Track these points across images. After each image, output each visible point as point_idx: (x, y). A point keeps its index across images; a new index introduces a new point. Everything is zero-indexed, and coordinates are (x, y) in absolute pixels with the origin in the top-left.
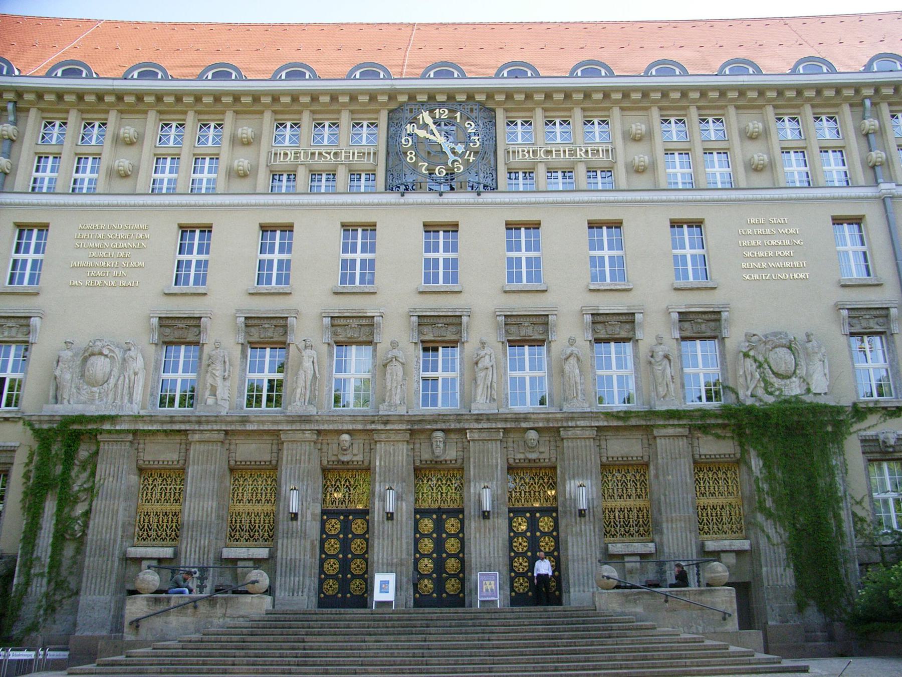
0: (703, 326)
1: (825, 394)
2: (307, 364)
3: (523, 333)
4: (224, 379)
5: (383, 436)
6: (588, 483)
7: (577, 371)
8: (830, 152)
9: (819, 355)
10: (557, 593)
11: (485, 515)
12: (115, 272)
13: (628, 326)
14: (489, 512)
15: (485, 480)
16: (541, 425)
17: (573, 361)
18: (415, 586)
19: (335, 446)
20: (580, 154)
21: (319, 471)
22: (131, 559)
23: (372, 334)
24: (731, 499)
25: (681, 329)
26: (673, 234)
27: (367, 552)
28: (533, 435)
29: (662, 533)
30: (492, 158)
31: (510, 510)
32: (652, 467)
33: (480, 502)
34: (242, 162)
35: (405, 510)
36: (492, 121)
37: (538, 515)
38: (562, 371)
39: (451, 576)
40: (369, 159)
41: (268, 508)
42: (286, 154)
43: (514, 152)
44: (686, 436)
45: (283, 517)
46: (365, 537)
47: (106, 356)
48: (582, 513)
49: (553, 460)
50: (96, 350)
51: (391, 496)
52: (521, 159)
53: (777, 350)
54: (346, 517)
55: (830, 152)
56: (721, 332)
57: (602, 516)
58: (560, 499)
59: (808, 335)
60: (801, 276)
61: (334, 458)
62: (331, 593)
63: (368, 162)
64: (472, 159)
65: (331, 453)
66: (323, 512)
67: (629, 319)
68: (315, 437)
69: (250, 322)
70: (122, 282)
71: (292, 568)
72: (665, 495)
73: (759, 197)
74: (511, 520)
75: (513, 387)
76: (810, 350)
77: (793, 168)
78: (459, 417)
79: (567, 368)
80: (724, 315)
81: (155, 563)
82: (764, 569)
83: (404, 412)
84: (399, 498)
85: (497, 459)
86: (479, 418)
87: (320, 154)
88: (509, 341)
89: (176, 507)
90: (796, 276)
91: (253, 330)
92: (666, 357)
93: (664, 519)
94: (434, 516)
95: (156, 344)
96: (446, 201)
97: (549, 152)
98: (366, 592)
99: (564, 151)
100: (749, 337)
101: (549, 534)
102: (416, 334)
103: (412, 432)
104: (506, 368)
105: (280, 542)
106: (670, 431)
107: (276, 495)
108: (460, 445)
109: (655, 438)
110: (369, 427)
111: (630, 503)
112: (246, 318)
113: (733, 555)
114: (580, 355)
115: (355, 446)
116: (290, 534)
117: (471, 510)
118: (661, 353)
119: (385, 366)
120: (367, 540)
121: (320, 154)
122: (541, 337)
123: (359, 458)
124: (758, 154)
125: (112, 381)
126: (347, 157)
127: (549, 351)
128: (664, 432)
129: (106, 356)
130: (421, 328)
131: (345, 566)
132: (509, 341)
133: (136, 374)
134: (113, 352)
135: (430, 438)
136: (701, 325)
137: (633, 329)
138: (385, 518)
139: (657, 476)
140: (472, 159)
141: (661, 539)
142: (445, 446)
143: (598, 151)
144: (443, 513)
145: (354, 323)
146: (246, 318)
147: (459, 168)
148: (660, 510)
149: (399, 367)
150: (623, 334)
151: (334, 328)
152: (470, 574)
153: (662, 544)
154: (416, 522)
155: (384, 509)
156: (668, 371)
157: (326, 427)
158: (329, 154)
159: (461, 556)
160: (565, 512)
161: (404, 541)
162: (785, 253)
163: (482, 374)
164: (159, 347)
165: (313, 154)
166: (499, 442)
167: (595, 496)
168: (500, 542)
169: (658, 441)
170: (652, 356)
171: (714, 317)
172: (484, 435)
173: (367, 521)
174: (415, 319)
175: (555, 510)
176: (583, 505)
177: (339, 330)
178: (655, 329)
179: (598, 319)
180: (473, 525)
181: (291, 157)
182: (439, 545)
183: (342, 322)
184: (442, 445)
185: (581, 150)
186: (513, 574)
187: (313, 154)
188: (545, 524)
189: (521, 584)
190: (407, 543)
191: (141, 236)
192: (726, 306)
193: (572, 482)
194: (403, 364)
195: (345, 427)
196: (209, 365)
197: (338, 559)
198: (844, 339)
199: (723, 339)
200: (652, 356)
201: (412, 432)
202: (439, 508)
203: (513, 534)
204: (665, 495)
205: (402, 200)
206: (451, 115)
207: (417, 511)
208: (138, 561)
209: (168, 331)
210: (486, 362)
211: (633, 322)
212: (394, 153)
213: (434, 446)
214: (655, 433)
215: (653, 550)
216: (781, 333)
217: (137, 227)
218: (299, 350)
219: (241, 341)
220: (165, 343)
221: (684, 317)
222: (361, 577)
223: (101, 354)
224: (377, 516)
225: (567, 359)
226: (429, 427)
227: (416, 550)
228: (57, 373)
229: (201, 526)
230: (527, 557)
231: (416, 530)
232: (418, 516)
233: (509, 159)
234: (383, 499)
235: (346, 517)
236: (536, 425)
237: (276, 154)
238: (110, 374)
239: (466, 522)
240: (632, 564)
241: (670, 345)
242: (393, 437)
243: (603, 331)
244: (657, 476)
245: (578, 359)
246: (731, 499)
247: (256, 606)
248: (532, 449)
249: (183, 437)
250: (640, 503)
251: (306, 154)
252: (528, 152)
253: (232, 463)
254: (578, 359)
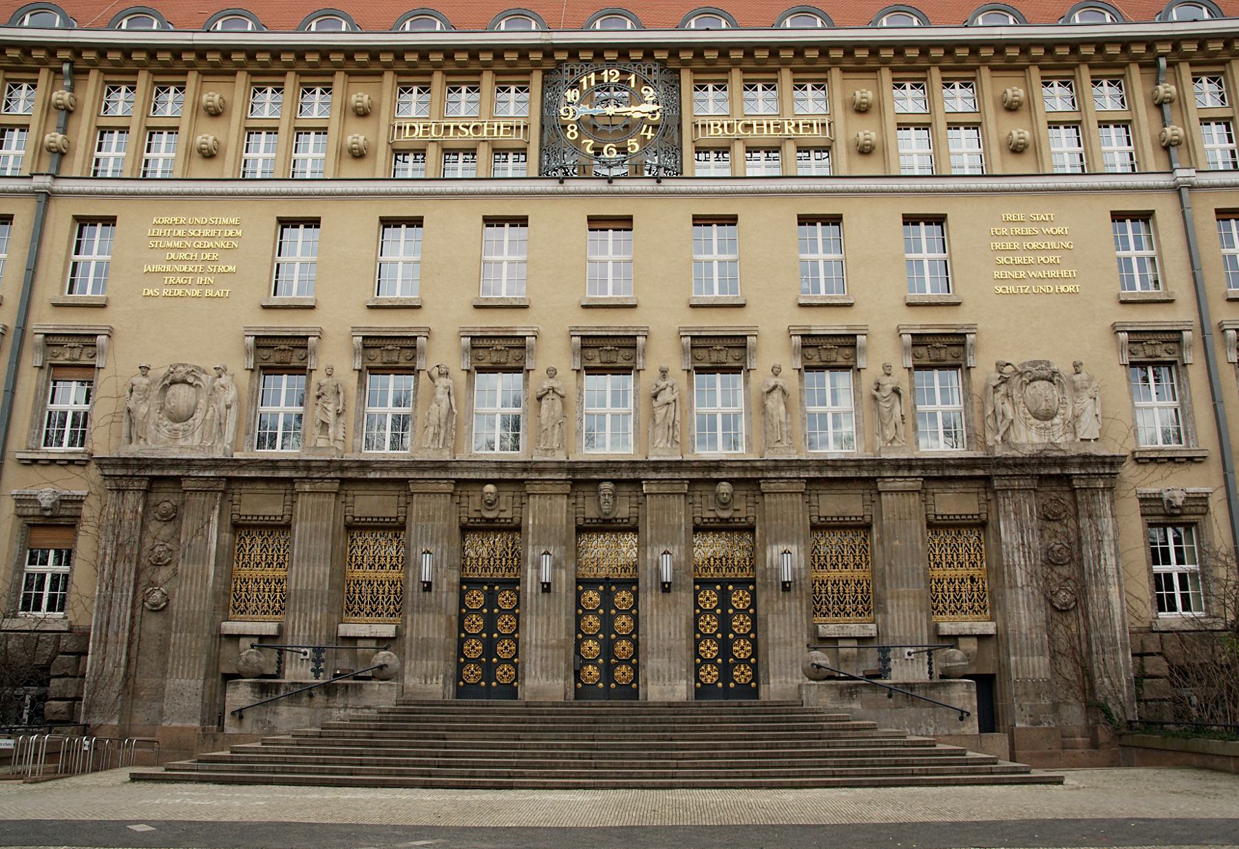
0: (943, 352)
1: (1096, 440)
2: (441, 395)
3: (714, 359)
4: (338, 415)
5: (537, 487)
6: (794, 549)
7: (782, 408)
8: (1112, 127)
9: (1090, 392)
10: (753, 684)
11: (666, 588)
12: (200, 280)
13: (847, 351)
14: (669, 584)
15: (660, 542)
16: (736, 475)
17: (776, 395)
18: (577, 674)
19: (478, 498)
20: (789, 129)
21: (457, 530)
22: (227, 636)
23: (523, 358)
24: (973, 571)
25: (914, 356)
26: (906, 233)
27: (517, 631)
28: (725, 488)
29: (886, 612)
30: (676, 134)
31: (696, 582)
32: (874, 529)
33: (658, 571)
34: (357, 135)
35: (564, 580)
36: (676, 84)
37: (731, 587)
38: (764, 406)
39: (621, 662)
40: (518, 135)
41: (394, 575)
42: (412, 128)
43: (704, 126)
44: (919, 492)
45: (413, 587)
46: (515, 613)
47: (191, 384)
48: (786, 587)
49: (751, 519)
50: (178, 377)
51: (546, 562)
52: (715, 134)
53: (1036, 383)
54: (491, 587)
55: (1112, 127)
56: (965, 359)
57: (811, 591)
58: (759, 568)
59: (1075, 366)
60: (1069, 289)
61: (476, 515)
62: (472, 681)
63: (515, 139)
64: (650, 135)
65: (473, 506)
66: (463, 581)
67: (848, 341)
69: (369, 343)
70: (209, 292)
71: (424, 648)
72: (890, 565)
73: (1017, 186)
74: (696, 594)
75: (701, 427)
76: (1078, 384)
77: (1062, 149)
78: (633, 465)
79: (769, 404)
80: (970, 338)
81: (255, 641)
82: (1013, 658)
83: (564, 459)
84: (556, 565)
85: (680, 517)
86: (656, 466)
87: (456, 128)
88: (696, 368)
89: (280, 573)
90: (1062, 289)
91: (372, 352)
92: (896, 391)
93: (889, 595)
94: (601, 588)
95: (252, 370)
96: (616, 189)
97: (748, 127)
99: (768, 126)
100: (1000, 366)
101: (745, 611)
102: (578, 359)
103: (575, 483)
104: (691, 403)
105: (409, 617)
106: (899, 485)
107: (405, 562)
109: (879, 493)
110: (519, 476)
111: (846, 574)
112: (365, 338)
113: (975, 640)
114: (786, 388)
115: (503, 498)
116: (423, 608)
117: (647, 580)
118: (889, 387)
119: (540, 399)
120: (517, 616)
121: (456, 128)
122: (737, 365)
123: (507, 514)
124: (1019, 130)
125: (199, 415)
126: (490, 132)
127: (746, 382)
128: (890, 485)
129: (191, 384)
130: (585, 351)
131: (490, 648)
132: (696, 368)
133: (228, 407)
134: (199, 379)
135: (597, 492)
136: (941, 350)
137: (855, 355)
138: (540, 590)
139: (881, 541)
140: (650, 135)
141: (885, 620)
142: (615, 501)
143: (812, 125)
144: (613, 584)
145: (500, 345)
146: (365, 338)
147: (633, 147)
148: (884, 584)
149: (558, 401)
150: (841, 361)
151: (475, 352)
152: (646, 659)
153: (885, 626)
154: (579, 595)
155: (538, 578)
156: (897, 410)
157: (465, 476)
158: (468, 127)
159: (634, 637)
160: (765, 585)
161: (563, 617)
162: (1050, 260)
163: (663, 411)
164: (256, 374)
165: (447, 128)
167: (802, 566)
168: (684, 621)
169: (883, 496)
170: (877, 390)
171: (958, 340)
172: (664, 488)
174: (578, 340)
175: (753, 582)
176: (787, 576)
177: (481, 352)
178: (884, 355)
179: (810, 341)
180: (649, 598)
181: (419, 132)
182: (607, 624)
183: (486, 343)
184: (611, 500)
185: (790, 124)
186: (698, 660)
187: (447, 128)
188: (740, 599)
189: (709, 673)
190: (567, 621)
191: (231, 233)
192: (972, 327)
193: (775, 547)
194: (562, 397)
195: (490, 476)
196: (318, 397)
197: (482, 640)
198: (1122, 372)
199: (969, 368)
200: (877, 390)
201: (575, 483)
202: (607, 579)
203: (699, 612)
204: (890, 565)
205: (561, 188)
206: (624, 77)
207: (579, 582)
208: (235, 638)
209: (266, 352)
210: (665, 397)
211: (854, 346)
212: (551, 128)
213: (602, 501)
214: (880, 485)
215: (874, 633)
216: (1041, 362)
217: (225, 221)
218: (432, 378)
219: (358, 366)
220: (262, 368)
221: (919, 340)
222: (509, 661)
223: (184, 382)
224: (530, 586)
225: (769, 392)
226: (595, 477)
227: (578, 630)
228: (131, 405)
229: (311, 597)
230: (717, 640)
231: (578, 604)
232: (581, 588)
233: (697, 135)
234: (538, 566)
235: (491, 587)
237: (399, 128)
238: (196, 407)
239: (641, 596)
240: (848, 649)
241: (900, 377)
242: (550, 489)
243: (1141, 354)
244: (881, 541)
245: (784, 392)
246: (973, 571)
247: (381, 696)
248: (725, 505)
249: (289, 486)
250: (859, 574)
251: (438, 127)
252: (722, 126)
253: (349, 518)
254: (784, 392)
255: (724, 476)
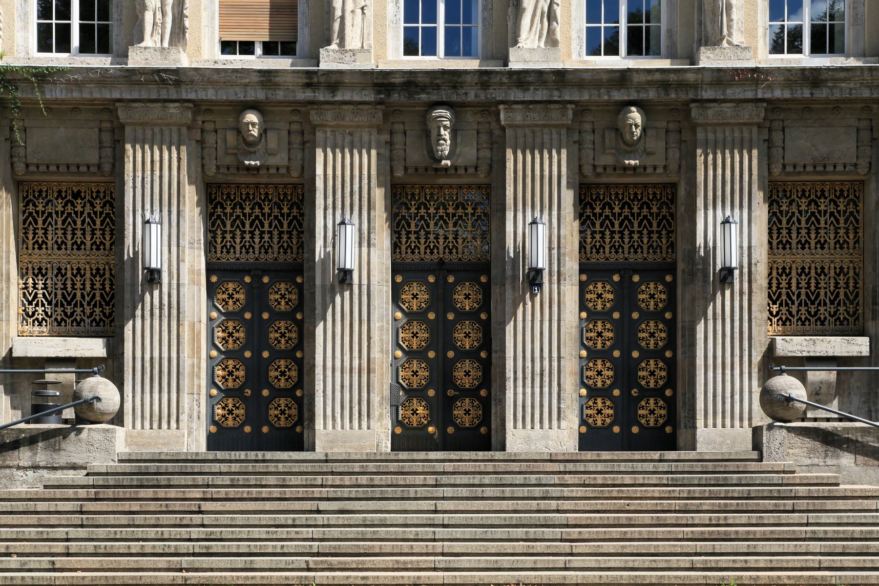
41: (98, 259)
54: (257, 278)
58: (682, 246)
61: (228, 160)
68: (189, 115)
86: (522, 78)
98: (300, 421)
108: (484, 137)
120: (300, 324)
144: (450, 272)
166: (563, 131)
173: (300, 287)
175: (672, 269)
202: (441, 262)
222: (288, 393)
235: (257, 278)
236: (643, 96)
239: (495, 290)
255: (634, 96)
